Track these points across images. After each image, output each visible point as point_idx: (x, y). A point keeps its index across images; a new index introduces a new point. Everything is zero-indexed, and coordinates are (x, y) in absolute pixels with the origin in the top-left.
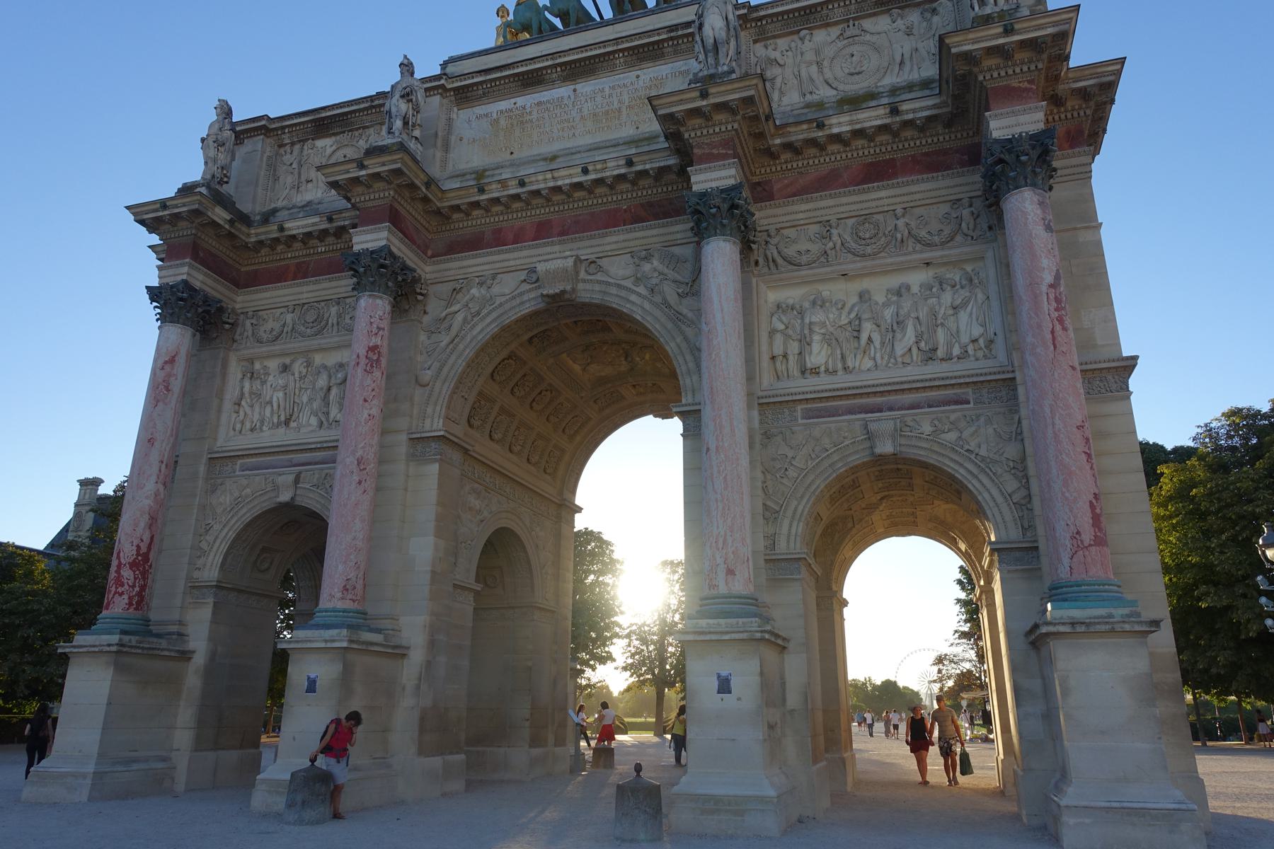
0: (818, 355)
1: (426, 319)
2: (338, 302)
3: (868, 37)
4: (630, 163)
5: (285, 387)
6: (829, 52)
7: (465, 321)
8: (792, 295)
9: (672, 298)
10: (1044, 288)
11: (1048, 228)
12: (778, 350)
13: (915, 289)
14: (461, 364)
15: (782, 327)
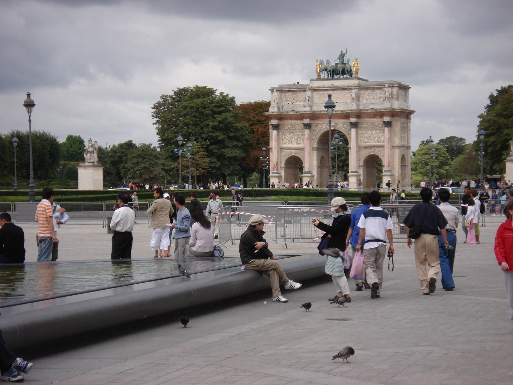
0: (366, 140)
1: (312, 129)
2: (298, 125)
3: (375, 93)
4: (342, 111)
5: (290, 137)
6: (370, 94)
7: (319, 131)
8: (363, 132)
9: (348, 131)
10: (387, 140)
11: (388, 132)
12: (361, 139)
13: (378, 133)
14: (318, 137)
15: (361, 136)
